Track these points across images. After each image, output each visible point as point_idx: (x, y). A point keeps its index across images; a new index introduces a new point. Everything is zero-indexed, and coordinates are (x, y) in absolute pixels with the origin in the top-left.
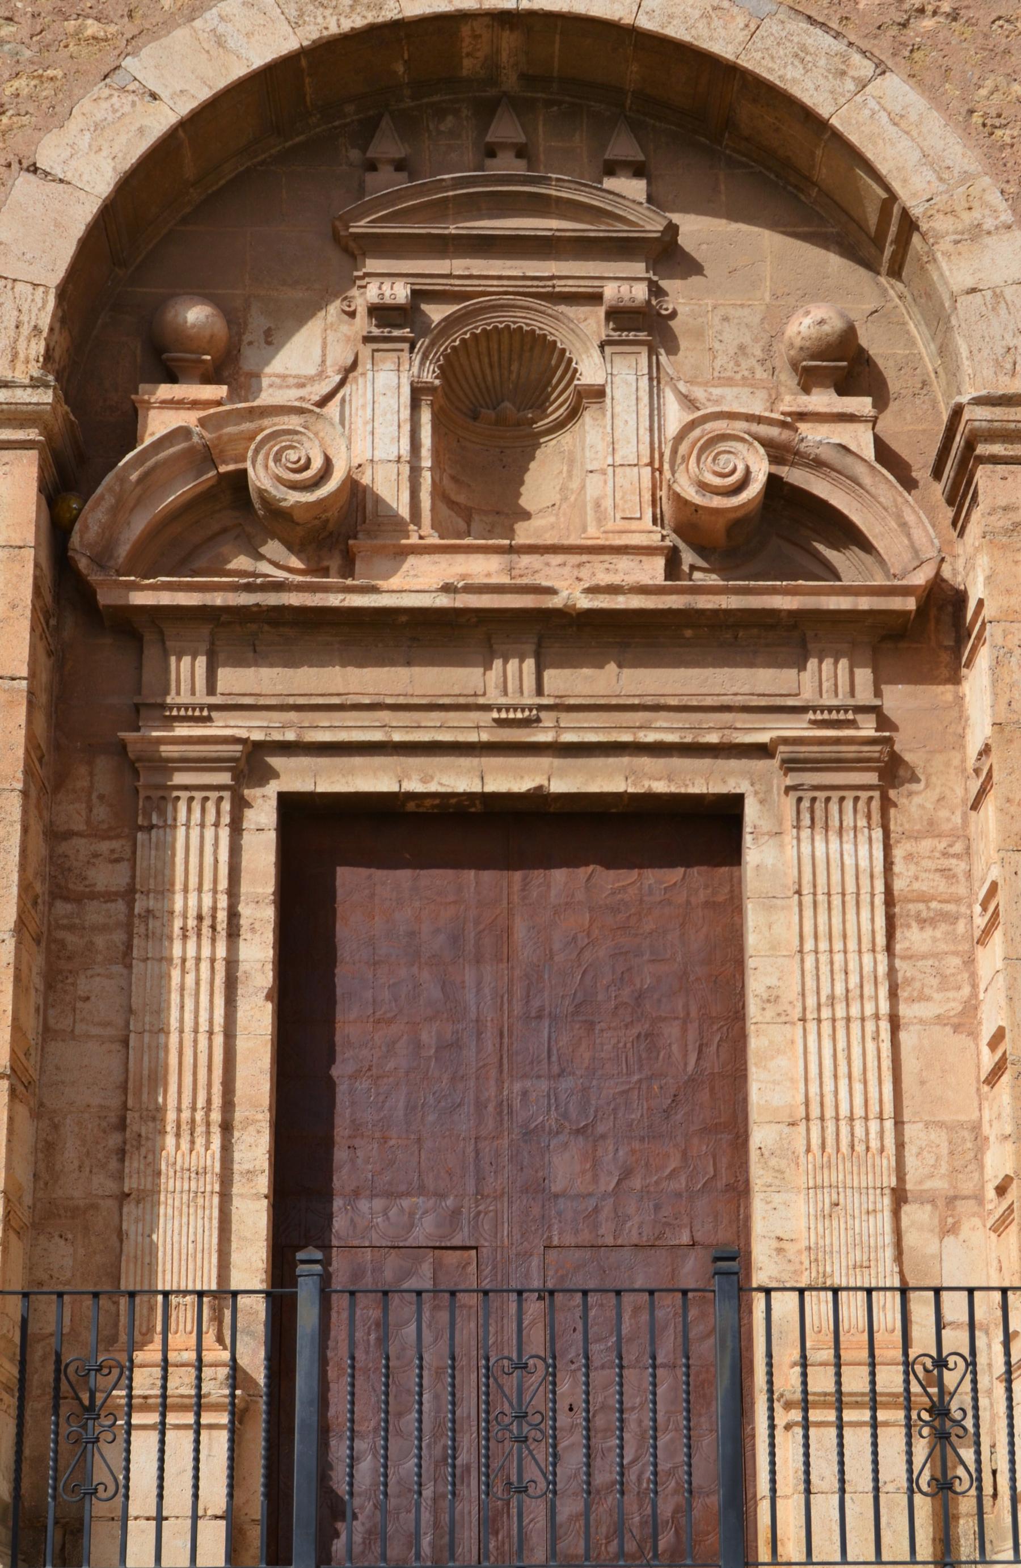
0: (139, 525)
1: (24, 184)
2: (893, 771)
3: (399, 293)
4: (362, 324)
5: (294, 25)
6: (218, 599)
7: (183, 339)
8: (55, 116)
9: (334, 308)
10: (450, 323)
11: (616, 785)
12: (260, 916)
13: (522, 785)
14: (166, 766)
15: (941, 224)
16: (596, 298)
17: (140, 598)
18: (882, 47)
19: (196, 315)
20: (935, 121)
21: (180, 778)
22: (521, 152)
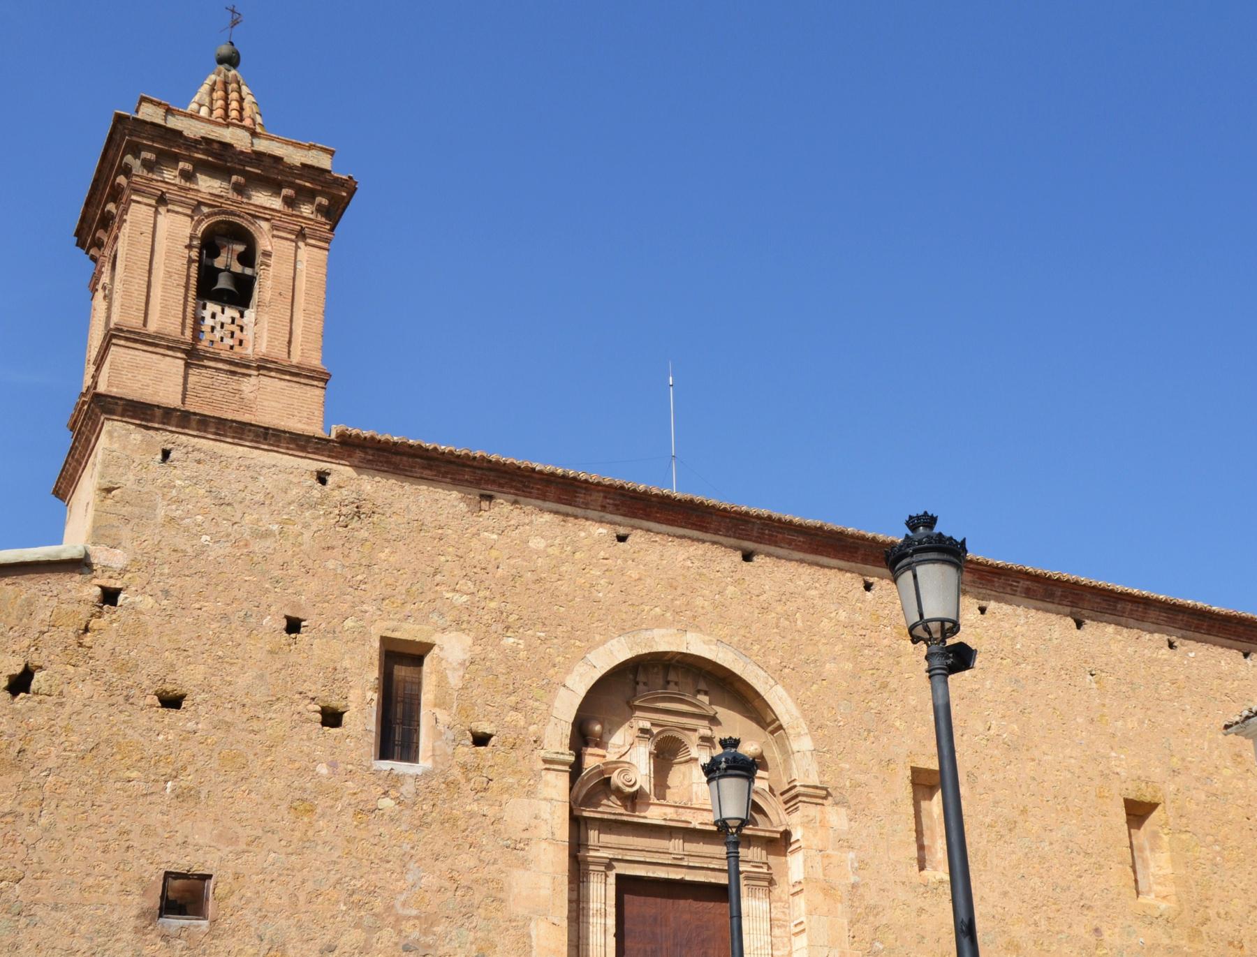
0: (584, 792)
1: (562, 691)
2: (771, 882)
3: (647, 725)
4: (635, 732)
5: (631, 649)
6: (606, 816)
7: (593, 734)
8: (569, 671)
9: (627, 724)
10: (659, 733)
11: (702, 879)
12: (612, 911)
13: (678, 877)
14: (588, 864)
15: (790, 731)
16: (695, 730)
17: (585, 814)
18: (776, 676)
19: (598, 728)
20: (789, 701)
21: (591, 867)
22: (676, 684)
